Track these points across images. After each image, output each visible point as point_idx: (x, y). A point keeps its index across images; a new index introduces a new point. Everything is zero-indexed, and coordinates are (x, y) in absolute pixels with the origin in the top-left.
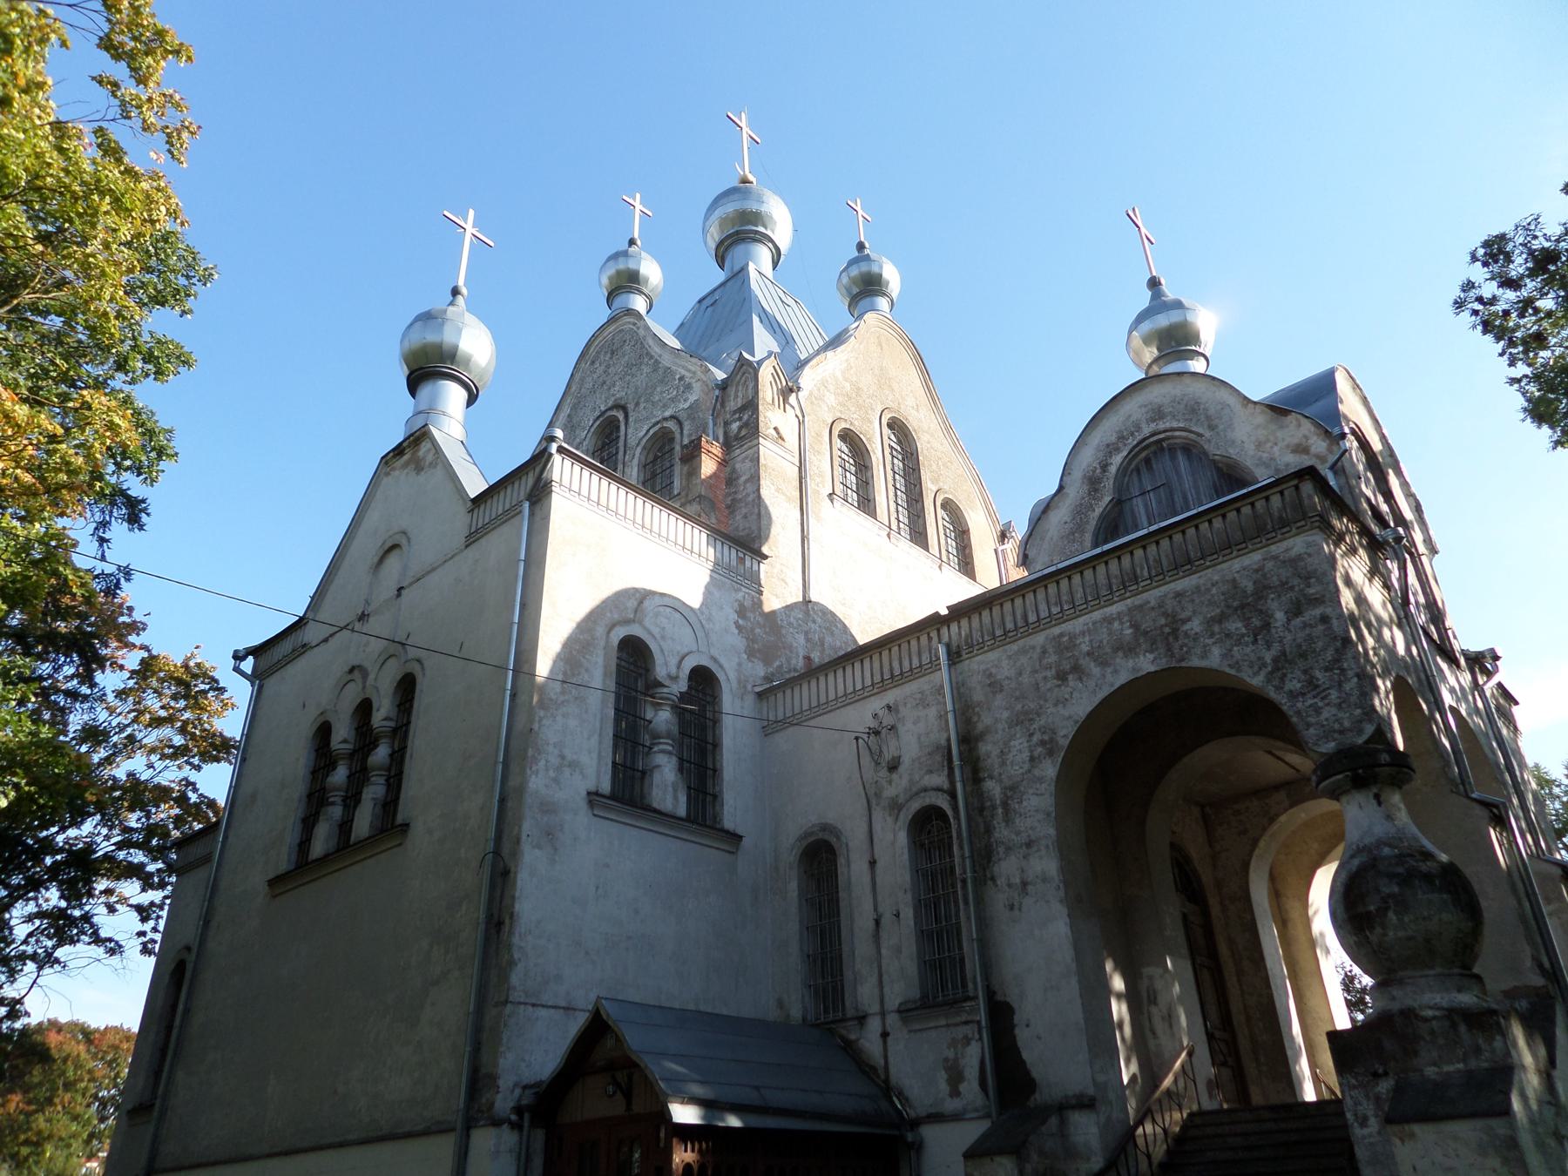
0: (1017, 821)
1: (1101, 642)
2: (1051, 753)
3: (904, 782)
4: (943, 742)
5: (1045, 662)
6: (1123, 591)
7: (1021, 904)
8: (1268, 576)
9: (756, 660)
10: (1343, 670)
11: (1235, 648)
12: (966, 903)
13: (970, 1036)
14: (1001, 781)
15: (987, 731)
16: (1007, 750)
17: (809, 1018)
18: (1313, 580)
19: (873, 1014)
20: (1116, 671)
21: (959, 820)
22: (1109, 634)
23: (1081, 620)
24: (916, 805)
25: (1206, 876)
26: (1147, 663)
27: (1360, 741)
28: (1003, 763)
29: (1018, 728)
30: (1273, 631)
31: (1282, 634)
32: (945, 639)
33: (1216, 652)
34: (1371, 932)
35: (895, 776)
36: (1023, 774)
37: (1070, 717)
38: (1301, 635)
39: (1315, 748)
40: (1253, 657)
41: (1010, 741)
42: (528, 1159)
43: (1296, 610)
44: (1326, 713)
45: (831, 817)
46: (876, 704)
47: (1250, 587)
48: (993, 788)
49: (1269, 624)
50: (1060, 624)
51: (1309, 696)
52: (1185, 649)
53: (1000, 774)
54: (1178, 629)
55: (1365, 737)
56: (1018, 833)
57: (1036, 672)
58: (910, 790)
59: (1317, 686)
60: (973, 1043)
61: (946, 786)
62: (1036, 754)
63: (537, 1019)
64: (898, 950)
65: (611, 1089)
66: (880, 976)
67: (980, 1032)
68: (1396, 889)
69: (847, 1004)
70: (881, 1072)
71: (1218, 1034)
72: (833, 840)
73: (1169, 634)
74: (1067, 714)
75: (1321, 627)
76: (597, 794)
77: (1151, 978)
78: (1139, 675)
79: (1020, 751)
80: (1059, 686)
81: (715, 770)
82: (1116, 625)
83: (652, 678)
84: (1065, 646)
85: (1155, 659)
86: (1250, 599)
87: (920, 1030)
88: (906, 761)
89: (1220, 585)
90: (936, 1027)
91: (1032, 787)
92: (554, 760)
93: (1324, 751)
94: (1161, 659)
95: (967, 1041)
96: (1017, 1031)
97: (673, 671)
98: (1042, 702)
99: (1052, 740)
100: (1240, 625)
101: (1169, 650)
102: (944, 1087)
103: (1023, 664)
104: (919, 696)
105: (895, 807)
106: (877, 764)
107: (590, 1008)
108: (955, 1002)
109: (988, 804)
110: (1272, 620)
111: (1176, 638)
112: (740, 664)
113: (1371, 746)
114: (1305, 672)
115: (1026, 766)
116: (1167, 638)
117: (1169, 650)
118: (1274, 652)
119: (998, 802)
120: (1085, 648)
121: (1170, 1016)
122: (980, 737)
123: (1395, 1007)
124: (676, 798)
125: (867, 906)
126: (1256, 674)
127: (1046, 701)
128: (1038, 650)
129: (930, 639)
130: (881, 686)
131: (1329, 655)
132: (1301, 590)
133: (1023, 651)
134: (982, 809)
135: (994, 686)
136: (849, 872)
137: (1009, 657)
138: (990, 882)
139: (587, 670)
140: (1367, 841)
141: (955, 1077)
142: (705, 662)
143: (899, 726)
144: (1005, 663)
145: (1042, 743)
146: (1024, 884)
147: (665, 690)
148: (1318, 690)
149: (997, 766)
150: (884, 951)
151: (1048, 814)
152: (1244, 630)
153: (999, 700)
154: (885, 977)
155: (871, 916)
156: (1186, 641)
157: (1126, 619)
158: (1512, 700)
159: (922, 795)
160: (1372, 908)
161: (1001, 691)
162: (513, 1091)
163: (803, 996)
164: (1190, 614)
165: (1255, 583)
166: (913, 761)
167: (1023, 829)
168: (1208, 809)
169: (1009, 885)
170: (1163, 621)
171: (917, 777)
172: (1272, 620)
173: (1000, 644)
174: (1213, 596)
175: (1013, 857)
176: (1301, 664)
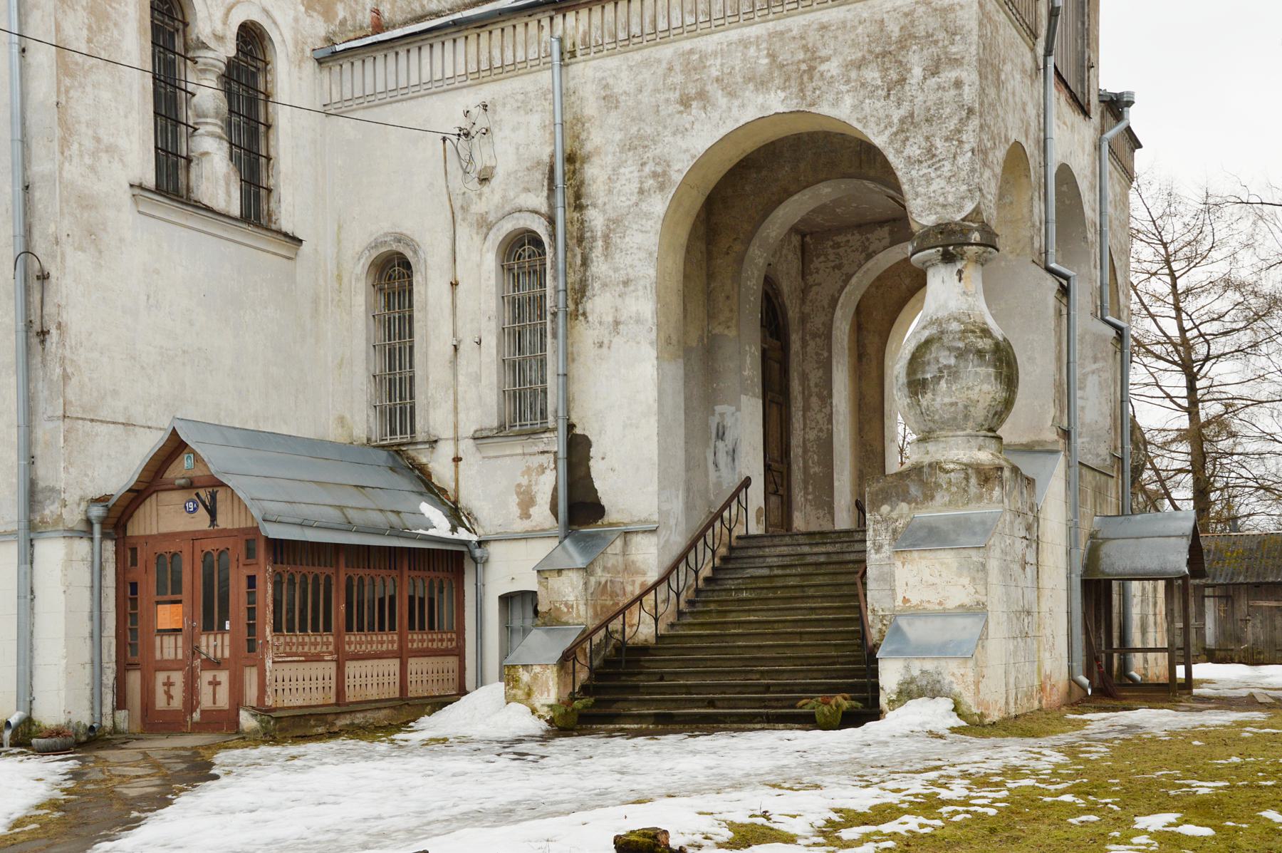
0: (617, 256)
1: (733, 68)
2: (662, 187)
3: (497, 198)
4: (546, 159)
5: (669, 81)
6: (766, 12)
7: (611, 341)
8: (916, 23)
9: (315, 14)
10: (961, 142)
11: (867, 101)
12: (555, 336)
13: (545, 465)
14: (604, 212)
15: (597, 151)
16: (615, 177)
17: (373, 439)
18: (958, 37)
19: (447, 439)
20: (743, 106)
21: (555, 249)
22: (744, 60)
23: (716, 37)
24: (508, 226)
25: (793, 313)
26: (776, 102)
27: (958, 218)
28: (610, 191)
29: (631, 154)
30: (907, 88)
31: (914, 93)
32: (558, 32)
33: (848, 101)
34: (923, 397)
35: (486, 189)
36: (629, 207)
37: (687, 151)
38: (933, 97)
39: (918, 219)
40: (881, 114)
41: (619, 167)
42: (101, 569)
43: (934, 70)
44: (937, 185)
45: (408, 227)
46: (470, 99)
47: (896, 34)
48: (596, 219)
49: (905, 80)
50: (692, 38)
51: (925, 164)
52: (818, 92)
53: (605, 204)
54: (814, 68)
55: (963, 215)
56: (616, 270)
57: (657, 91)
58: (503, 206)
59: (934, 156)
60: (548, 472)
61: (544, 208)
62: (646, 186)
63: (97, 435)
64: (477, 378)
65: (191, 505)
66: (456, 401)
67: (556, 462)
68: (952, 361)
69: (418, 427)
70: (451, 493)
71: (774, 465)
72: (409, 255)
73: (804, 71)
74: (684, 147)
75: (953, 92)
76: (141, 187)
77: (722, 415)
78: (766, 114)
79: (629, 180)
80: (681, 112)
81: (268, 158)
82: (752, 51)
83: (194, 37)
84: (694, 64)
85: (786, 98)
86: (893, 47)
87: (496, 457)
88: (500, 173)
89: (868, 25)
90: (512, 455)
91: (636, 223)
92: (89, 144)
93: (925, 223)
94: (791, 100)
95: (542, 469)
96: (592, 463)
97: (219, 28)
98: (660, 128)
99: (664, 173)
100: (877, 75)
101: (802, 90)
102: (516, 511)
103: (645, 80)
104: (521, 97)
105: (485, 225)
106: (466, 172)
107: (166, 426)
108: (535, 433)
109: (588, 234)
110: (909, 75)
111: (811, 79)
112: (296, 20)
113: (967, 223)
114: (927, 138)
115: (634, 198)
116: (801, 76)
117: (802, 90)
118: (903, 112)
119: (599, 234)
120: (715, 72)
121: (734, 451)
122: (586, 159)
123: (927, 460)
124: (228, 193)
125: (446, 329)
126: (881, 132)
127: (665, 127)
128: (664, 65)
129: (540, 27)
130: (478, 77)
131: (952, 124)
132: (945, 47)
133: (646, 63)
134: (580, 240)
135: (609, 100)
136: (426, 292)
137: (631, 68)
138: (581, 318)
139: (116, 25)
140: (940, 315)
141: (527, 502)
142: (256, 17)
143: (495, 130)
144: (624, 75)
145: (655, 175)
146: (617, 323)
147: (210, 54)
148: (934, 160)
149: (602, 194)
150: (461, 378)
151: (651, 254)
152: (879, 82)
153: (614, 118)
154: (461, 405)
155: (450, 342)
156: (820, 83)
157: (764, 45)
158: (1137, 144)
159: (517, 215)
160: (928, 376)
161: (616, 107)
162: (79, 505)
163: (368, 416)
164: (831, 52)
165: (901, 28)
166: (509, 175)
167: (622, 266)
168: (808, 239)
169: (600, 323)
170: (801, 56)
171: (512, 194)
172: (909, 75)
173: (622, 49)
174: (857, 35)
175: (608, 294)
176: (925, 129)
